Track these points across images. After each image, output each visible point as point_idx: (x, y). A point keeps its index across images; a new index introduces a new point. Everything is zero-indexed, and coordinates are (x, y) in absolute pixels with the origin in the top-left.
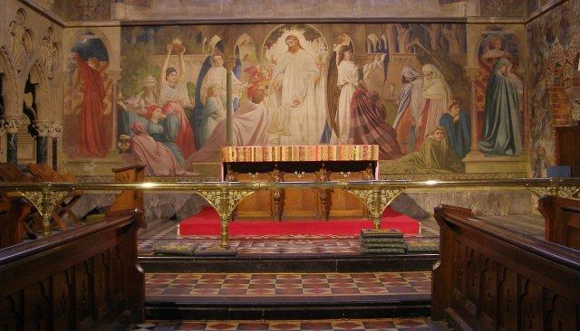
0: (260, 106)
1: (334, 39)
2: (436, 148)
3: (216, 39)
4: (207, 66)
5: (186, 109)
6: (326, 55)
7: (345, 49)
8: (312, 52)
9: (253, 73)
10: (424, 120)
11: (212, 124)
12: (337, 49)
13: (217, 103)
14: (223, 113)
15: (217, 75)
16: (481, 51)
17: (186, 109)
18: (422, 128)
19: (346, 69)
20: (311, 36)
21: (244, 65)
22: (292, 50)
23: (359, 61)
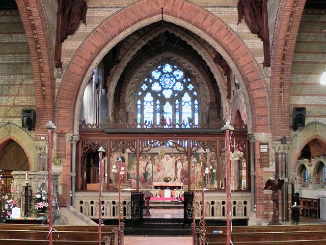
0: (160, 173)
1: (177, 157)
2: (200, 182)
3: (150, 157)
4: (148, 163)
5: (143, 173)
6: (175, 161)
7: (179, 160)
8: (172, 160)
9: (158, 165)
10: (197, 176)
11: (149, 177)
12: (177, 159)
13: (150, 172)
14: (151, 174)
15: (150, 165)
16: (210, 160)
17: (143, 173)
18: (197, 178)
19: (179, 164)
20: (171, 157)
21: (156, 163)
22: (167, 160)
23: (182, 162)
